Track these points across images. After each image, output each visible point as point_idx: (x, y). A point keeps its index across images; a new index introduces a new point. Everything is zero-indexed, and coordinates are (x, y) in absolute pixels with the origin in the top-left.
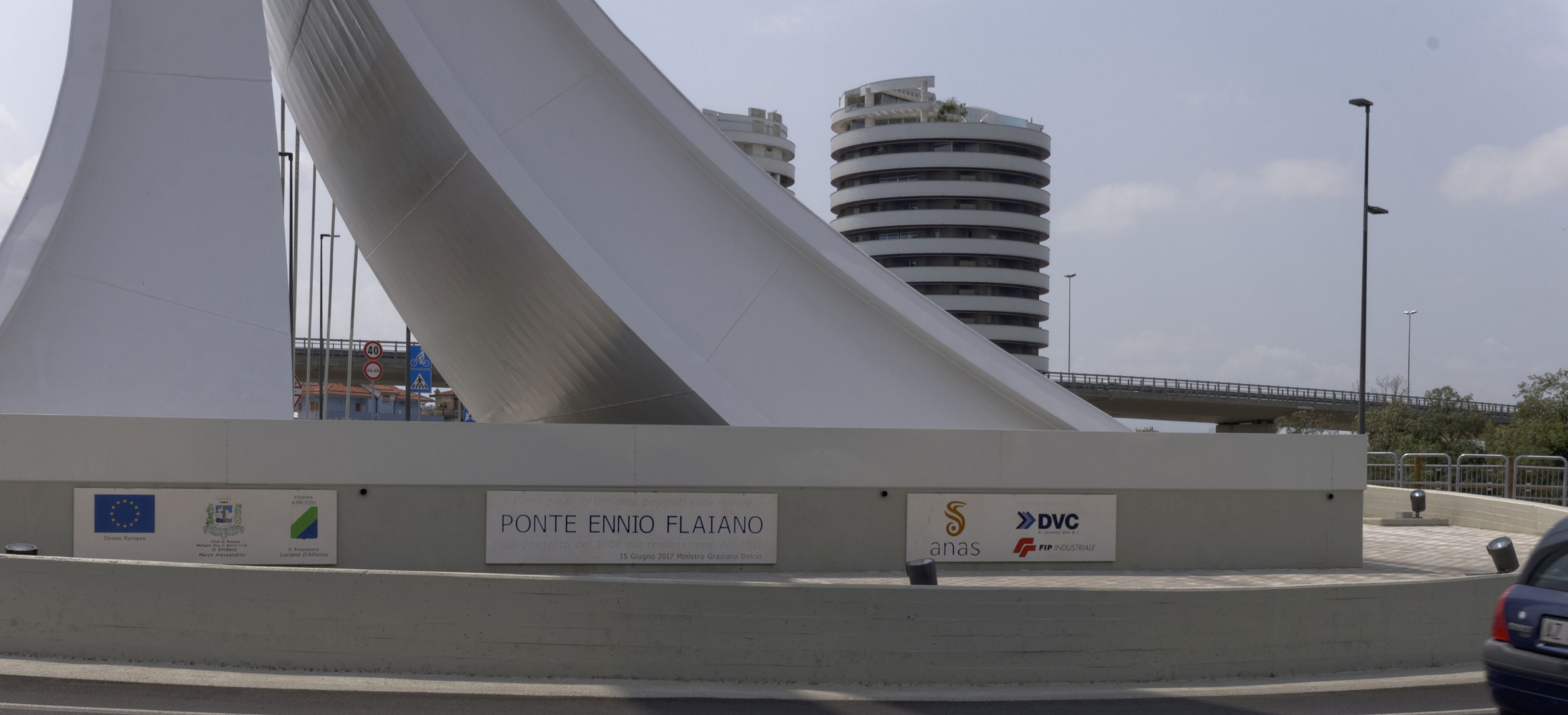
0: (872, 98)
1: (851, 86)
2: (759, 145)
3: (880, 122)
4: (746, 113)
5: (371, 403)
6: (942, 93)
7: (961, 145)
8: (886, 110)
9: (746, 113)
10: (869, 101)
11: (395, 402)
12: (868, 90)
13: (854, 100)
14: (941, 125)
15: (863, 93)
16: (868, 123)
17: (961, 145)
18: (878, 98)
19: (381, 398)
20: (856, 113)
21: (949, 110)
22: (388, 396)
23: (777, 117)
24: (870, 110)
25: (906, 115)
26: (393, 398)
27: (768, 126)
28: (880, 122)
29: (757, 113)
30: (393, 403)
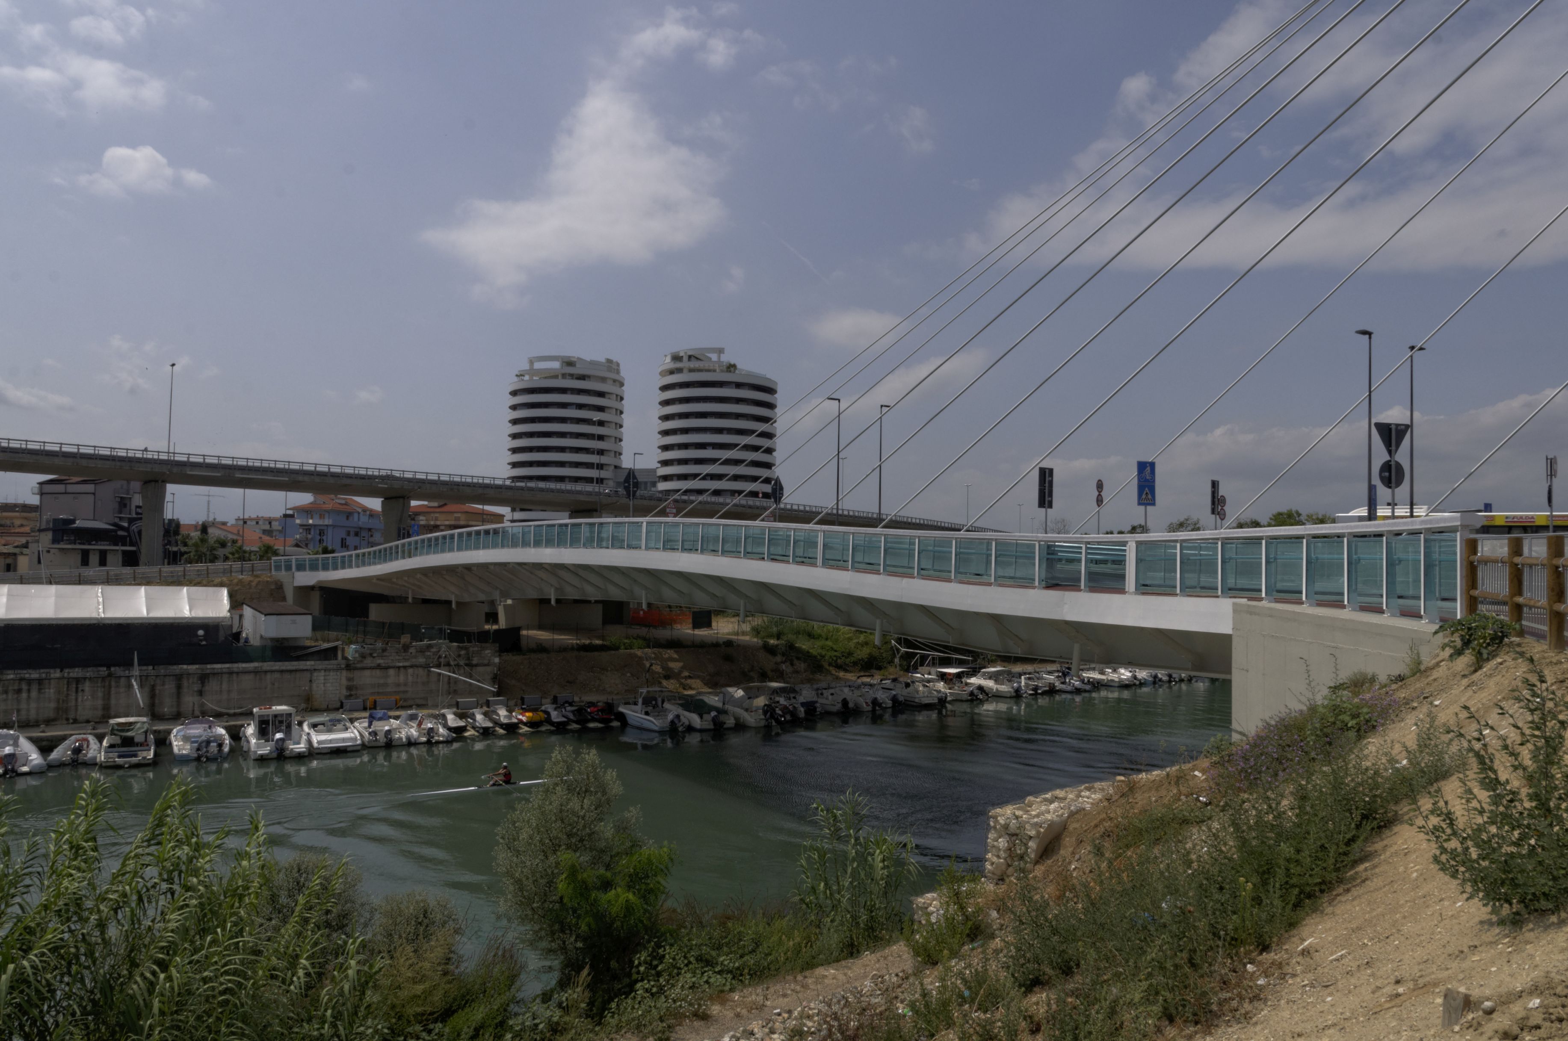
1: (675, 350)
3: (691, 370)
4: (603, 360)
5: (356, 515)
6: (726, 358)
7: (739, 385)
8: (694, 364)
9: (603, 360)
10: (685, 359)
13: (676, 358)
15: (681, 354)
16: (685, 371)
17: (739, 385)
18: (690, 357)
20: (679, 365)
21: (731, 367)
23: (618, 365)
24: (685, 364)
25: (707, 368)
26: (368, 513)
28: (691, 370)
29: (609, 361)
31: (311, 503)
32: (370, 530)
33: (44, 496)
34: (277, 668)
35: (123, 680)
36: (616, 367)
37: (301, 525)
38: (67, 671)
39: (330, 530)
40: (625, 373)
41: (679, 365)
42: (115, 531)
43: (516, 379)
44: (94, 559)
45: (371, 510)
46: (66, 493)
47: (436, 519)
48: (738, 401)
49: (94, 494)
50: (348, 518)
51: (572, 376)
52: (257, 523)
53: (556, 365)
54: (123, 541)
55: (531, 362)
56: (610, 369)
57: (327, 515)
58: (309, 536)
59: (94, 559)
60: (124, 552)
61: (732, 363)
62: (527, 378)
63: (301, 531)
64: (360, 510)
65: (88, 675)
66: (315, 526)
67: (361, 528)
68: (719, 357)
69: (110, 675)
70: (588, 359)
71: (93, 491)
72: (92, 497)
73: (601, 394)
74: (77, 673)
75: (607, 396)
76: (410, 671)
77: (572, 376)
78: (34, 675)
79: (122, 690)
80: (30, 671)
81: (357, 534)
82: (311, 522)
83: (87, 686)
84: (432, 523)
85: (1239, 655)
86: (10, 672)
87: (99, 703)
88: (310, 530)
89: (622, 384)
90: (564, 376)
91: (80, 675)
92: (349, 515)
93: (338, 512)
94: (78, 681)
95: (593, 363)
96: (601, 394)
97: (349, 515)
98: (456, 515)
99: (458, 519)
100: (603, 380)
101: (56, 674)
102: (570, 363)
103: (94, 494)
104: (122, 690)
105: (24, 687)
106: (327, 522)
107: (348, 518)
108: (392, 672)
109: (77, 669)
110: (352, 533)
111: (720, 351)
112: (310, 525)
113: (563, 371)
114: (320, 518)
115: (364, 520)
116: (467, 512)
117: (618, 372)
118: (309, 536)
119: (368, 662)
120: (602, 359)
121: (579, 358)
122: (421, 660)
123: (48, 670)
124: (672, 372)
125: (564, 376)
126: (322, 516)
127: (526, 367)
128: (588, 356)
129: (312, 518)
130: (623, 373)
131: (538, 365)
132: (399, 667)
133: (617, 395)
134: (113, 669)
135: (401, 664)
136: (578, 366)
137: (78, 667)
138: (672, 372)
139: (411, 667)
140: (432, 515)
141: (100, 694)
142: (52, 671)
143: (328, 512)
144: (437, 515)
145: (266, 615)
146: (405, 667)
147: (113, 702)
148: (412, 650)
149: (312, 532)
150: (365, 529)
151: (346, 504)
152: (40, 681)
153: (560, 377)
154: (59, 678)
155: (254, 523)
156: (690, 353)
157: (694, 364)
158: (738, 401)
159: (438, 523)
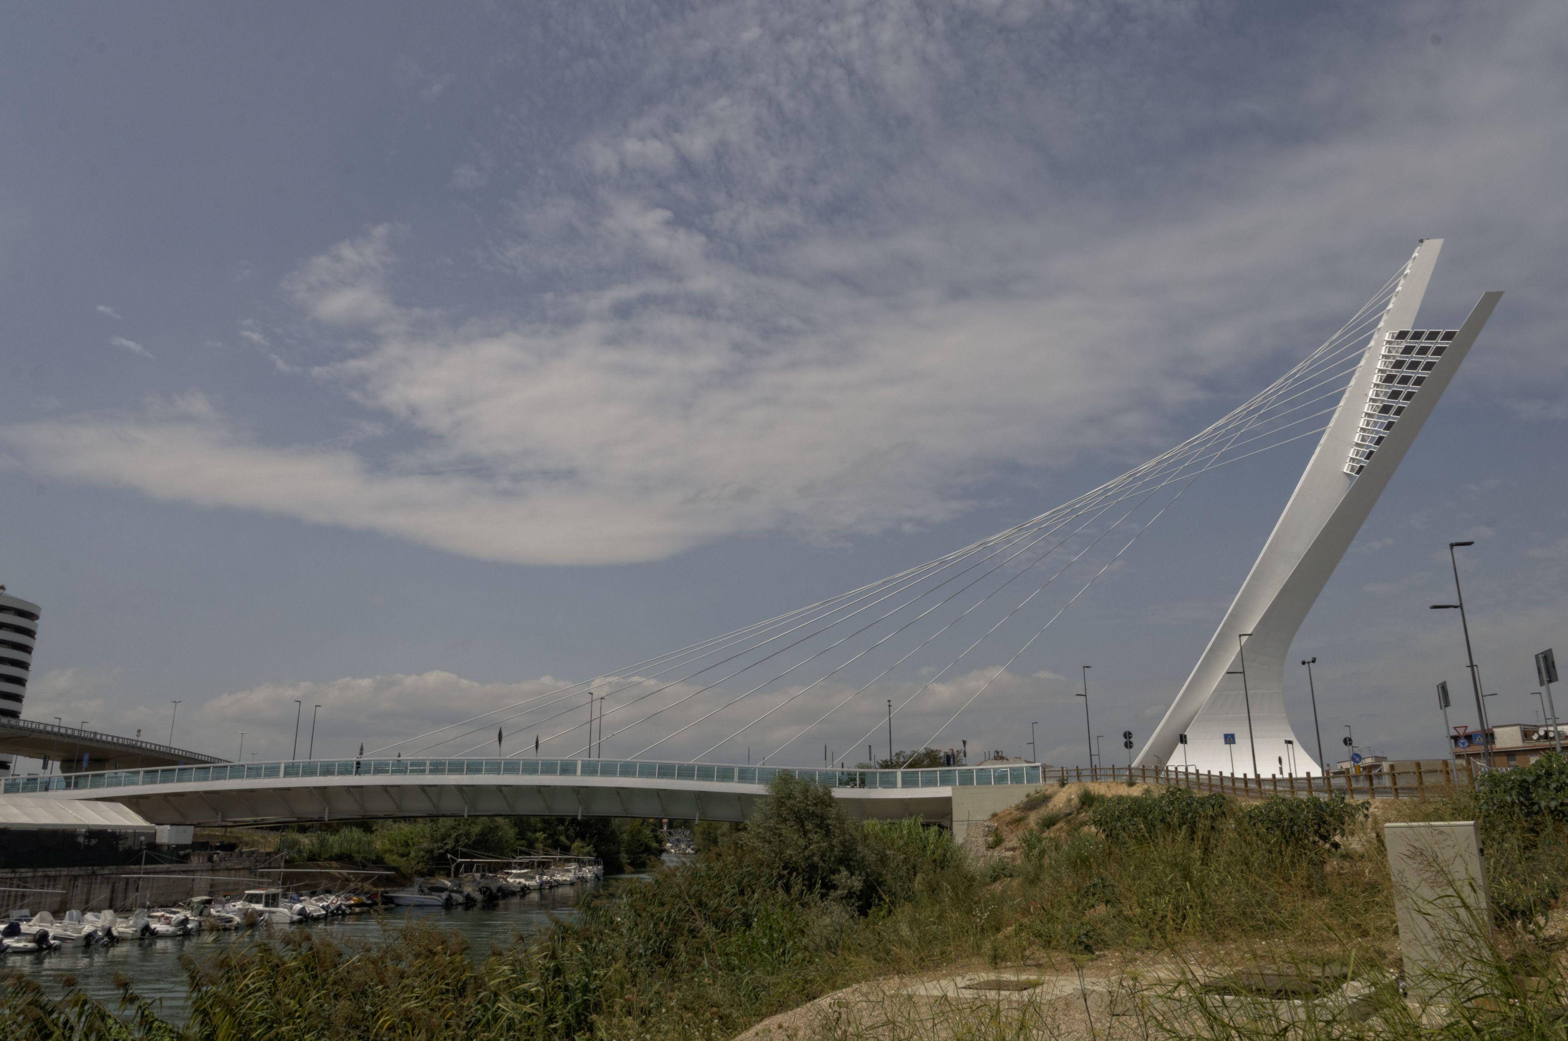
34: (177, 869)
35: (99, 877)
38: (71, 869)
65: (82, 873)
69: (93, 873)
74: (75, 871)
76: (242, 872)
78: (52, 872)
79: (98, 886)
80: (51, 869)
83: (80, 882)
85: (954, 801)
86: (40, 870)
87: (84, 897)
91: (77, 873)
94: (76, 878)
101: (64, 871)
104: (98, 886)
105: (46, 883)
108: (233, 872)
109: (76, 868)
119: (223, 865)
122: (247, 864)
123: (58, 869)
132: (236, 869)
134: (95, 868)
135: (238, 867)
137: (77, 866)
139: (244, 869)
141: (85, 890)
142: (62, 869)
145: (172, 825)
146: (240, 869)
147: (91, 897)
148: (244, 856)
152: (55, 878)
154: (66, 876)
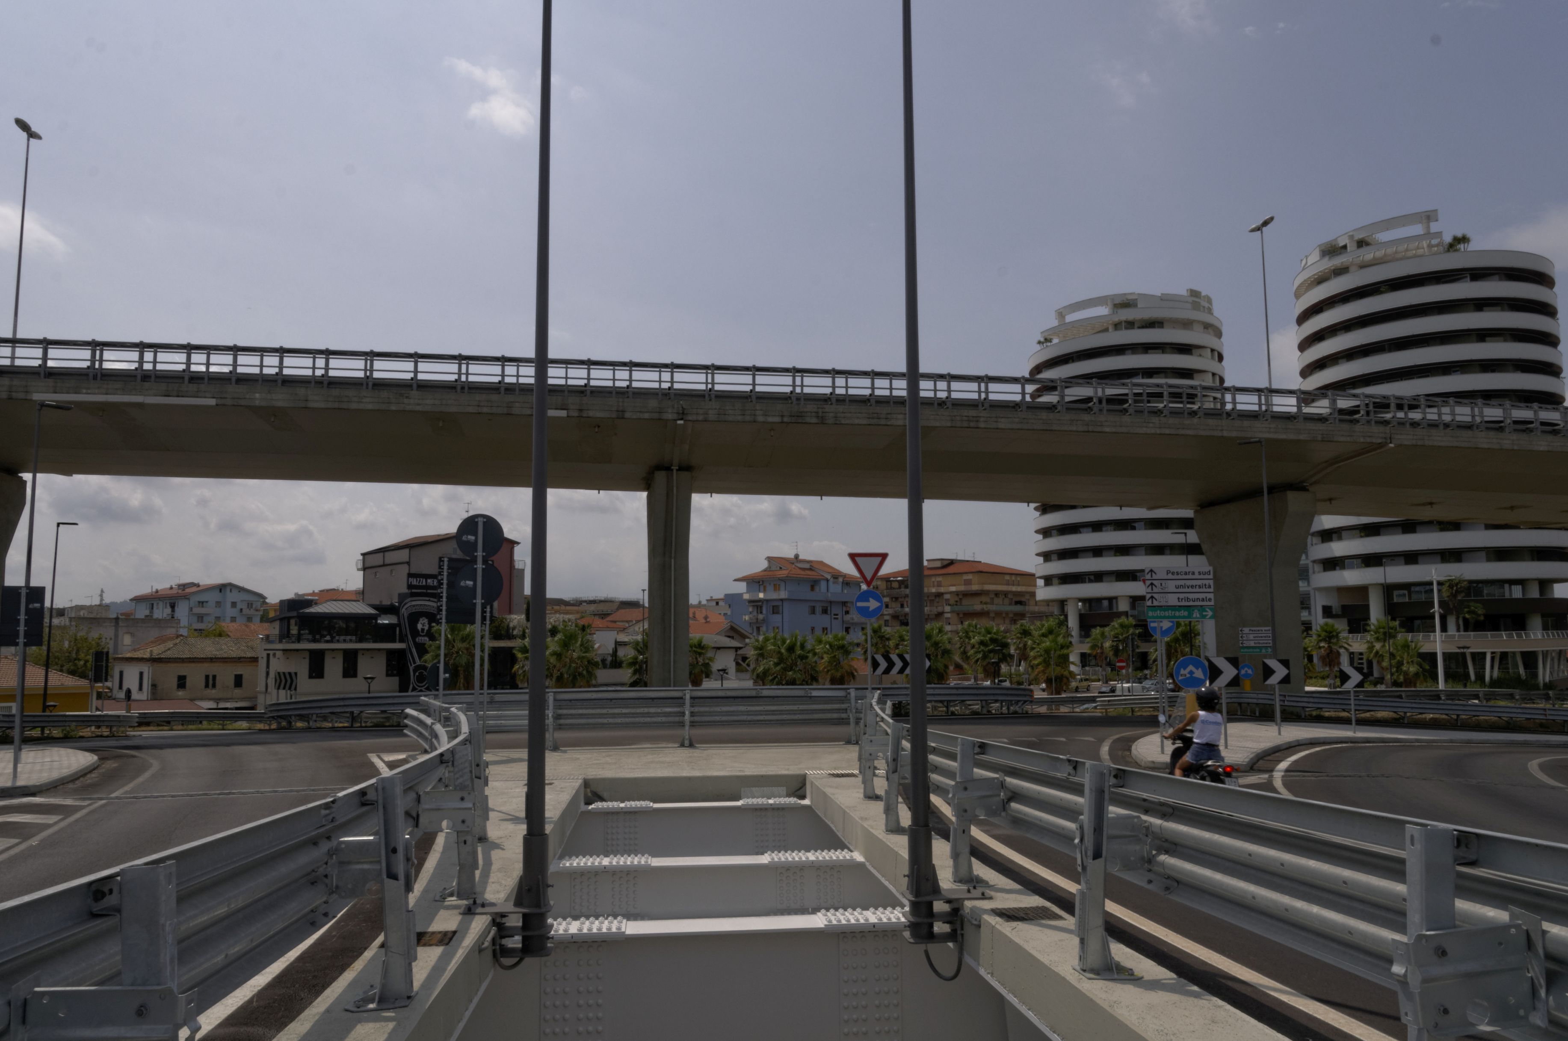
0: (1355, 245)
1: (1326, 237)
2: (1199, 322)
4: (1185, 293)
5: (823, 584)
7: (1478, 274)
9: (1185, 293)
11: (843, 583)
12: (1351, 237)
13: (1331, 250)
14: (1452, 255)
16: (1352, 269)
19: (832, 580)
20: (1338, 261)
22: (837, 578)
23: (1209, 300)
26: (841, 580)
27: (1204, 307)
29: (1194, 293)
30: (841, 584)
31: (765, 570)
32: (844, 603)
33: (367, 571)
36: (1206, 305)
37: (750, 601)
39: (786, 606)
40: (1221, 312)
41: (1338, 261)
42: (375, 617)
43: (1038, 347)
44: (333, 667)
45: (845, 576)
46: (384, 565)
47: (939, 585)
48: (1480, 304)
49: (408, 563)
50: (812, 588)
51: (1131, 325)
52: (717, 603)
53: (1103, 311)
54: (387, 634)
55: (1061, 314)
56: (1196, 306)
57: (782, 585)
58: (761, 617)
59: (333, 667)
60: (390, 653)
61: (1459, 235)
62: (1056, 341)
63: (751, 609)
64: (829, 577)
66: (767, 601)
67: (831, 602)
68: (1428, 227)
70: (1158, 292)
71: (406, 559)
72: (406, 567)
73: (1185, 349)
75: (1194, 351)
77: (1131, 325)
81: (825, 611)
82: (761, 595)
84: (934, 590)
88: (761, 607)
89: (1219, 334)
90: (1117, 326)
92: (814, 584)
93: (799, 581)
95: (1165, 298)
96: (1185, 349)
97: (814, 584)
98: (966, 577)
99: (968, 582)
100: (1187, 324)
102: (1125, 303)
103: (408, 563)
106: (783, 594)
107: (812, 588)
110: (818, 610)
111: (1429, 217)
112: (760, 601)
113: (1116, 319)
114: (775, 589)
115: (836, 588)
116: (981, 572)
117: (1210, 311)
118: (761, 617)
120: (1181, 290)
121: (1139, 294)
124: (1320, 280)
125: (1117, 326)
126: (776, 588)
127: (1055, 323)
128: (1157, 290)
129: (765, 591)
130: (1217, 312)
131: (1070, 318)
133: (1213, 350)
136: (1139, 306)
138: (1320, 280)
140: (933, 579)
143: (784, 580)
144: (939, 579)
149: (764, 611)
150: (837, 603)
151: (810, 569)
153: (1110, 330)
155: (714, 603)
156: (1359, 236)
157: (1368, 254)
158: (1480, 304)
159: (942, 590)
